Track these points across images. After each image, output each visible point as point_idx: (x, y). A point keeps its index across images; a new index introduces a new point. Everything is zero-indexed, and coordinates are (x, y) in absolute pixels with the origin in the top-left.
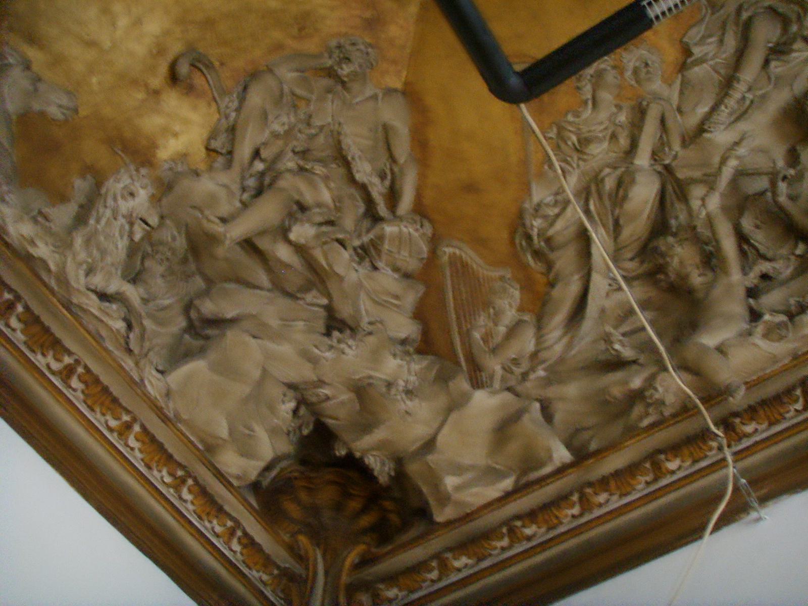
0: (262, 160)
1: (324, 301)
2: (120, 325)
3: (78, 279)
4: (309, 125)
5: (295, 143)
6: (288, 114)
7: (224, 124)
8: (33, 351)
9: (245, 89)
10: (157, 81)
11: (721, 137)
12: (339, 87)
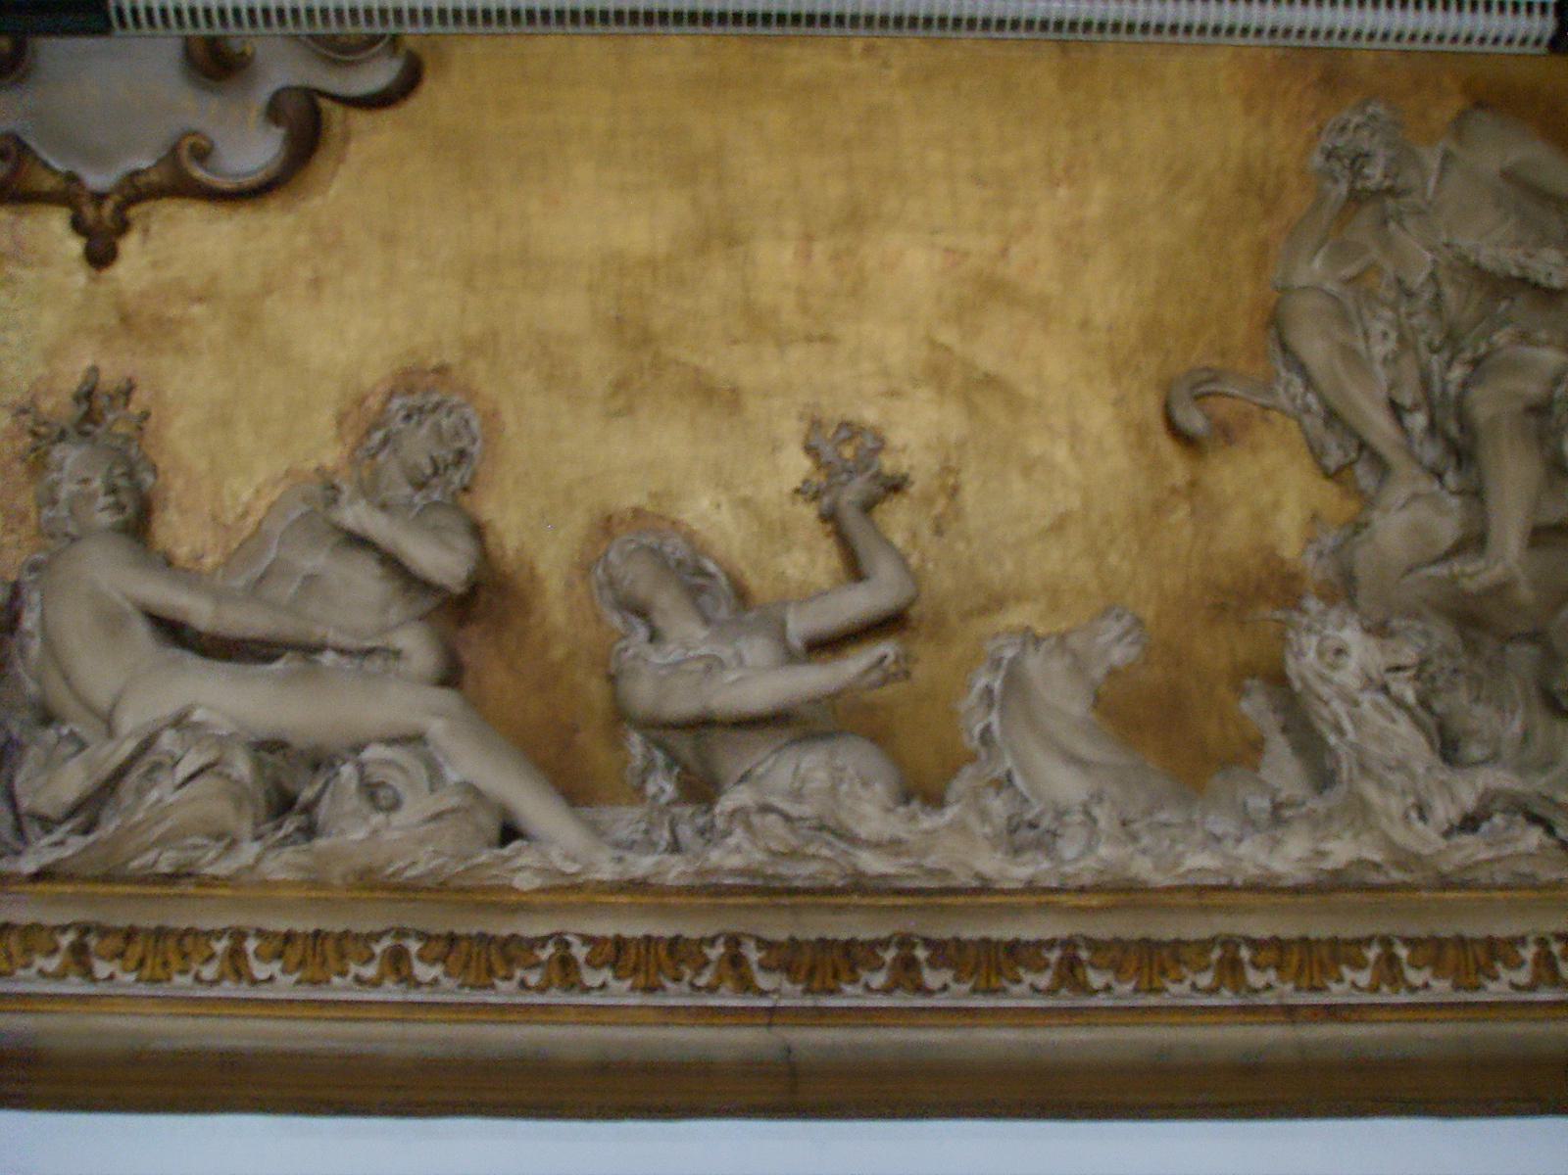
0: (1416, 407)
2: (1534, 837)
3: (1425, 839)
4: (1410, 295)
5: (1423, 338)
6: (1375, 316)
7: (1315, 424)
8: (1477, 988)
9: (1285, 347)
10: (1179, 470)
12: (1390, 203)
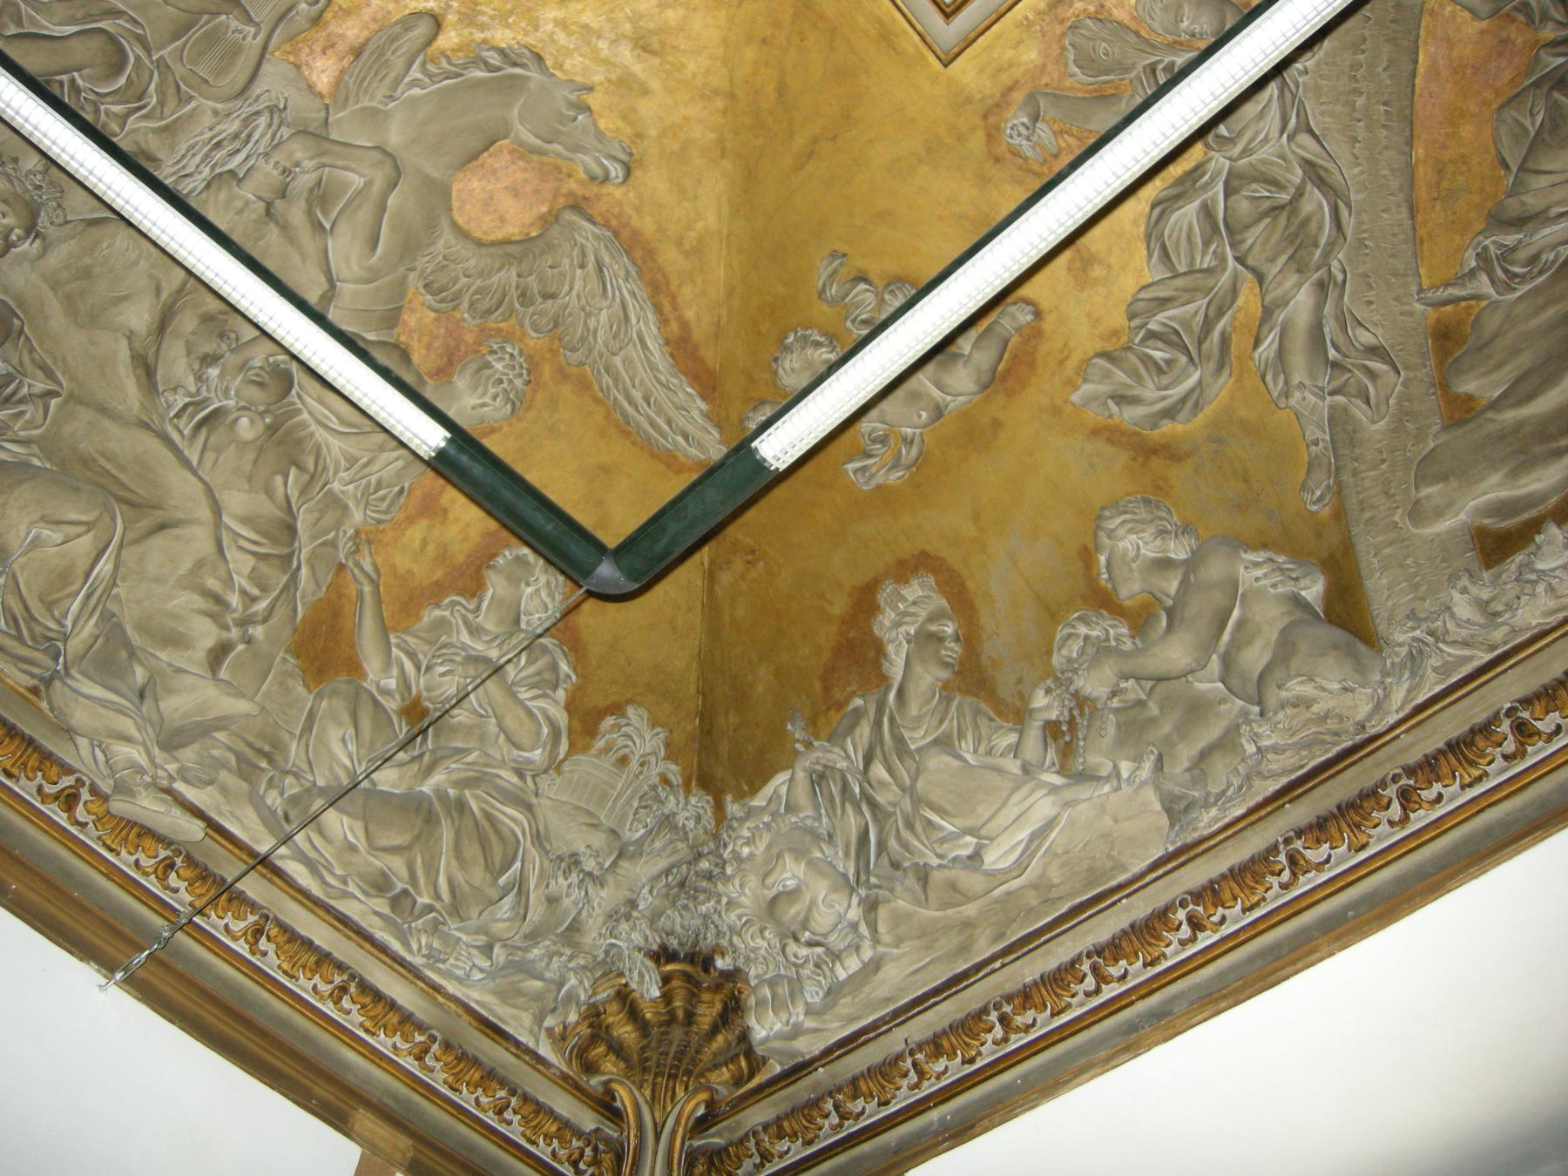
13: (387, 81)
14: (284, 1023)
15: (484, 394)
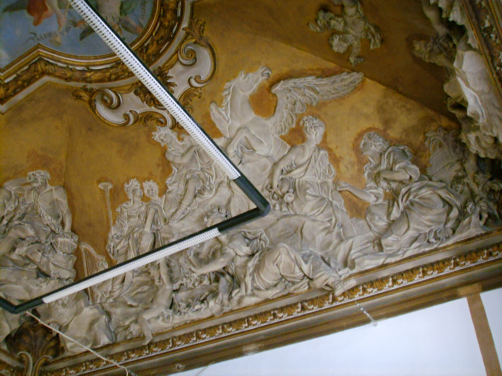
1: (36, 267)
11: (175, 224)
13: (223, 120)
14: (422, 291)
15: (313, 133)
